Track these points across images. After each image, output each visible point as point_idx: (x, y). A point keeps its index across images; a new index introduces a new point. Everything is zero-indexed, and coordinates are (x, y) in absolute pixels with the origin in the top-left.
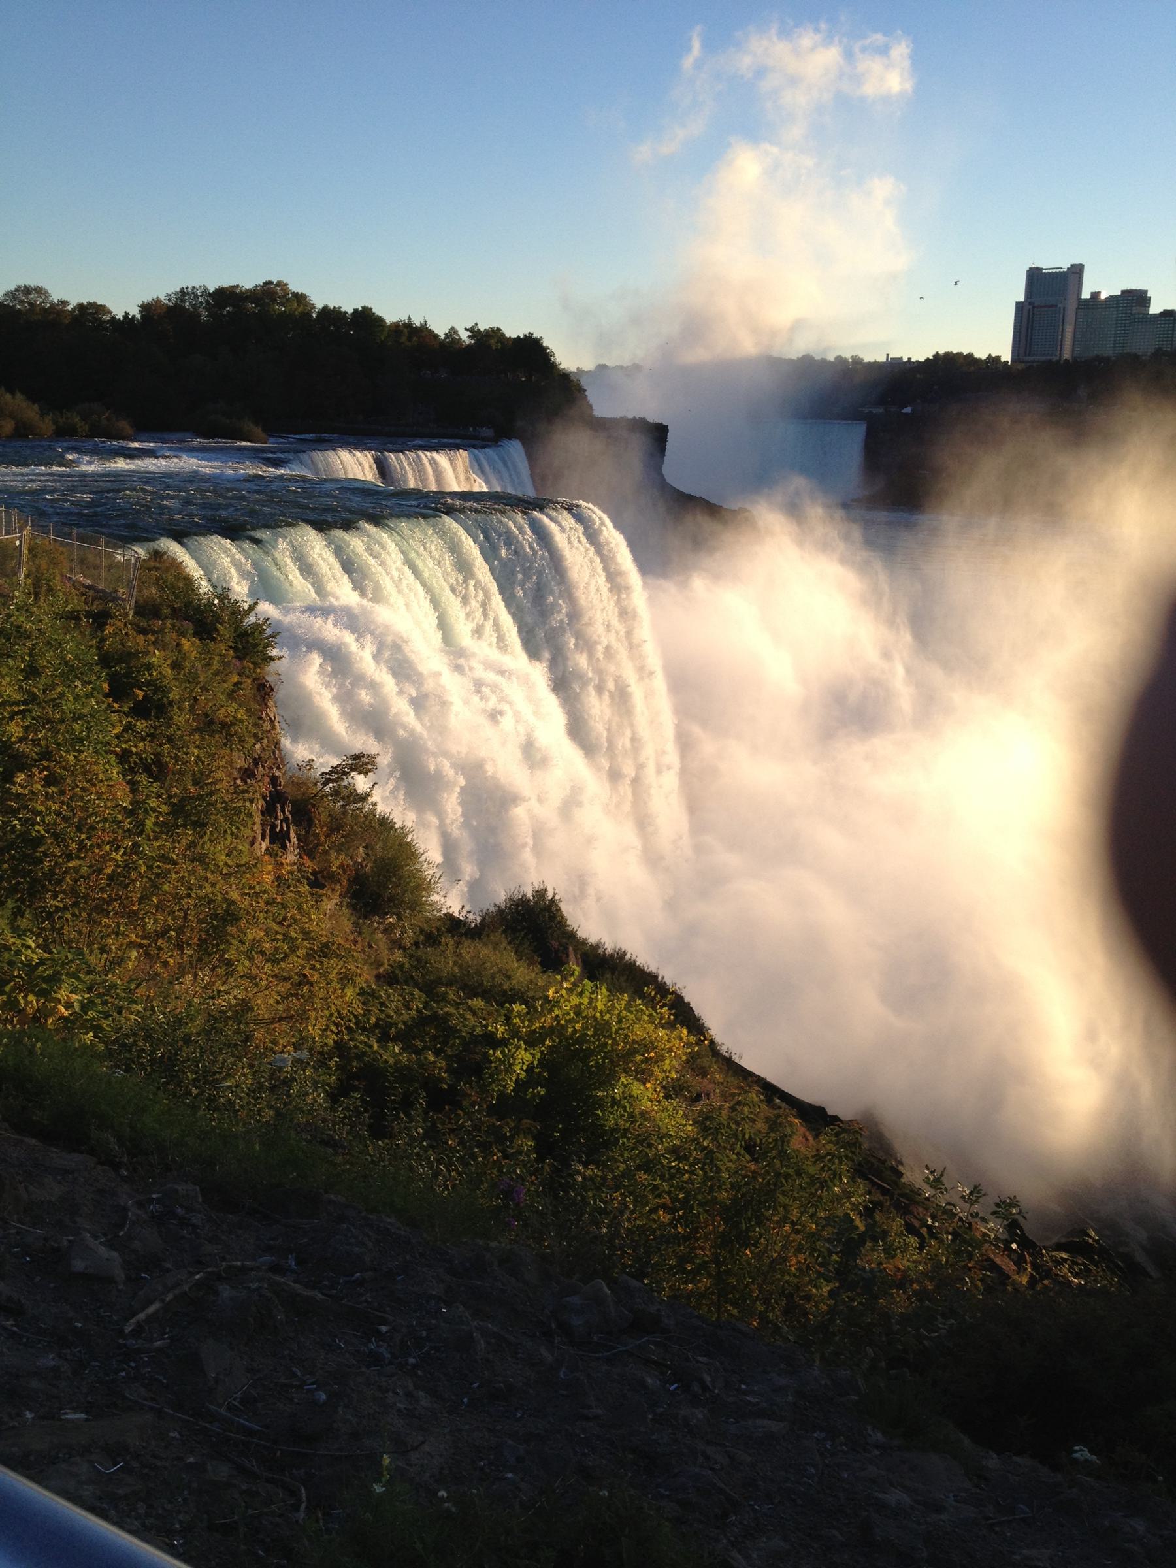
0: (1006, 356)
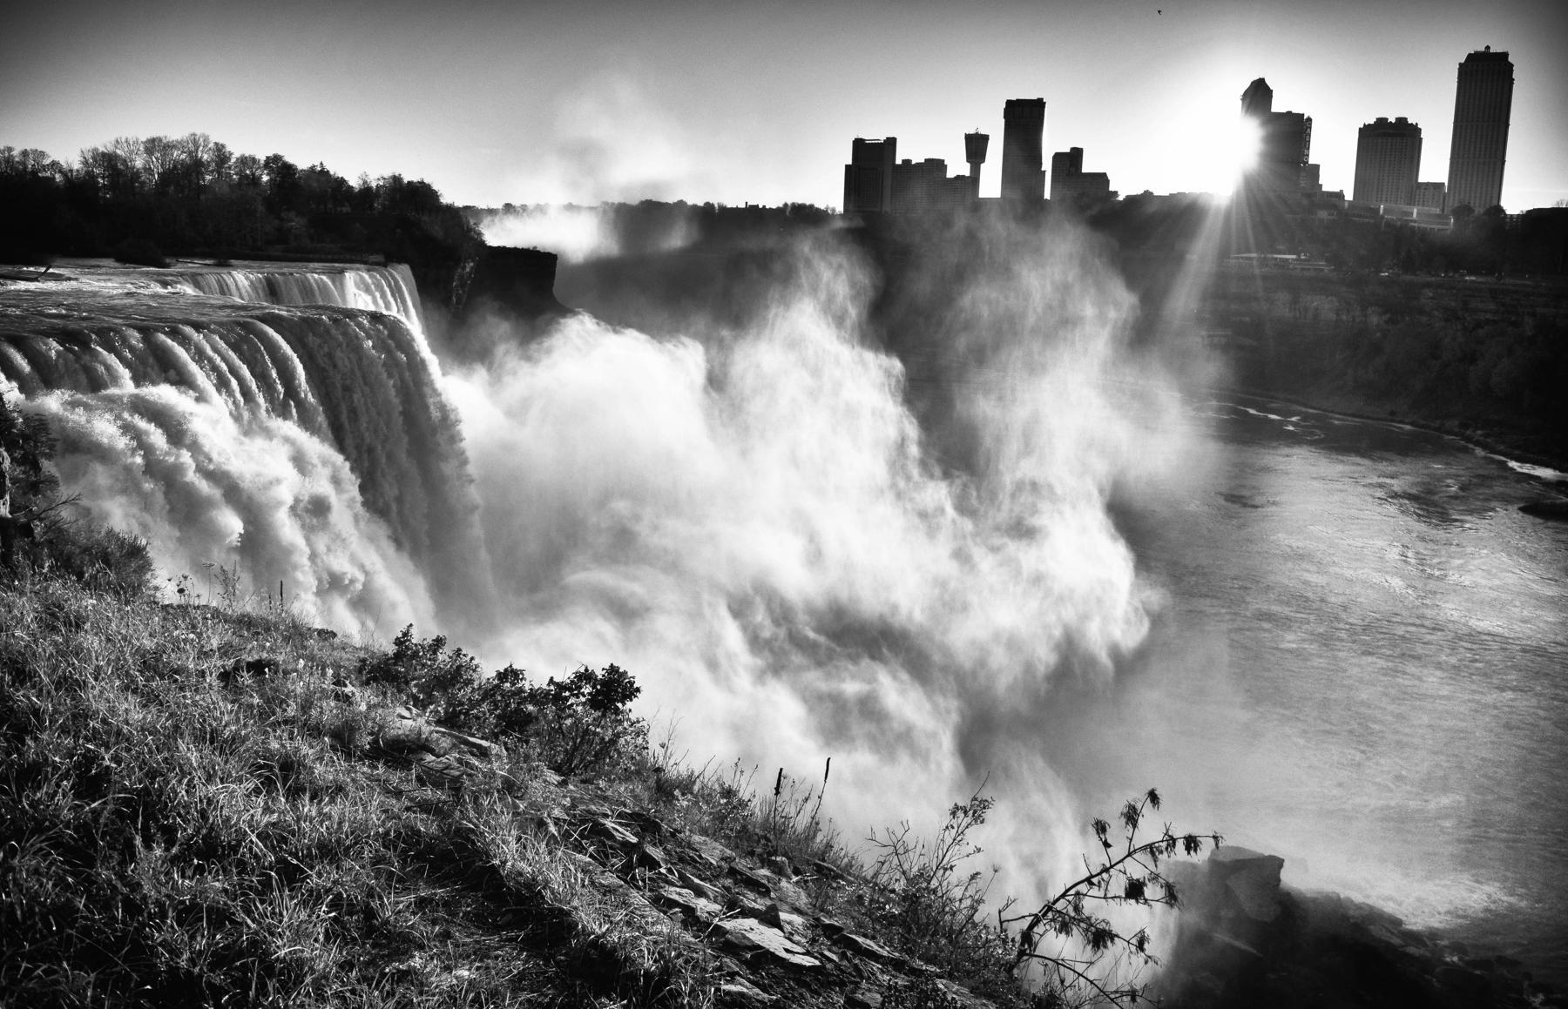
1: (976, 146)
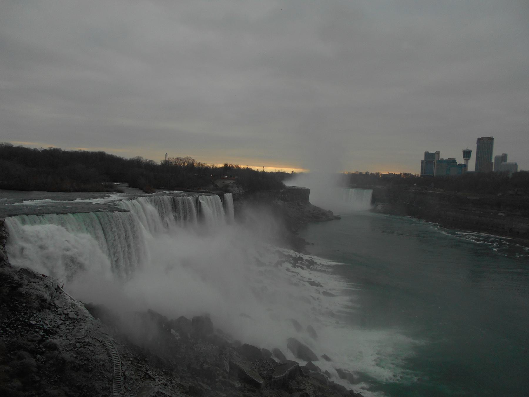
1: (467, 154)
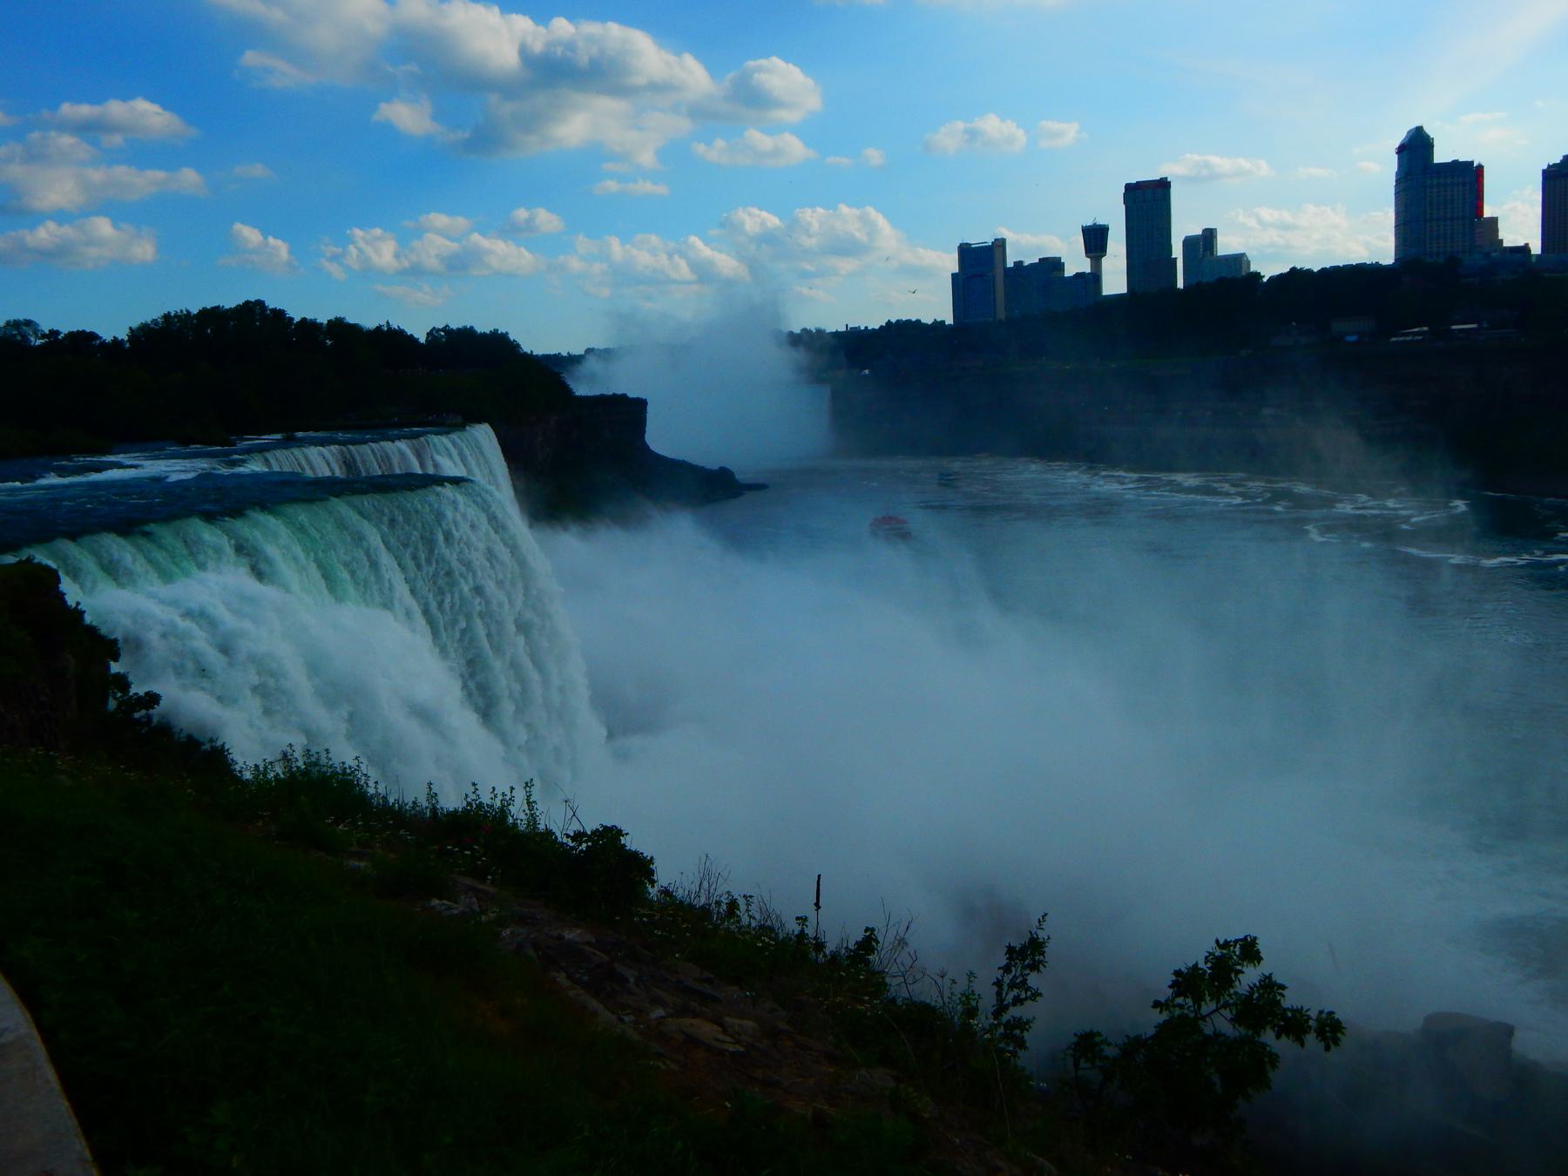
0: (949, 321)
1: (1095, 239)
